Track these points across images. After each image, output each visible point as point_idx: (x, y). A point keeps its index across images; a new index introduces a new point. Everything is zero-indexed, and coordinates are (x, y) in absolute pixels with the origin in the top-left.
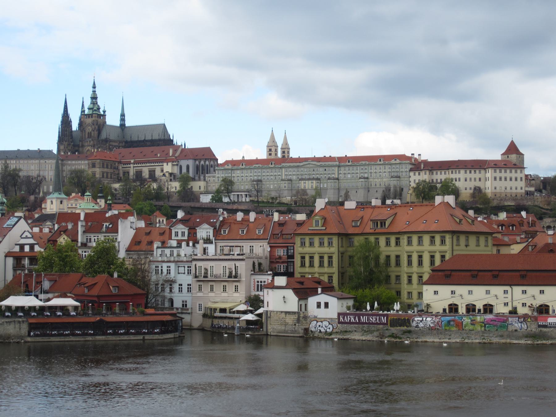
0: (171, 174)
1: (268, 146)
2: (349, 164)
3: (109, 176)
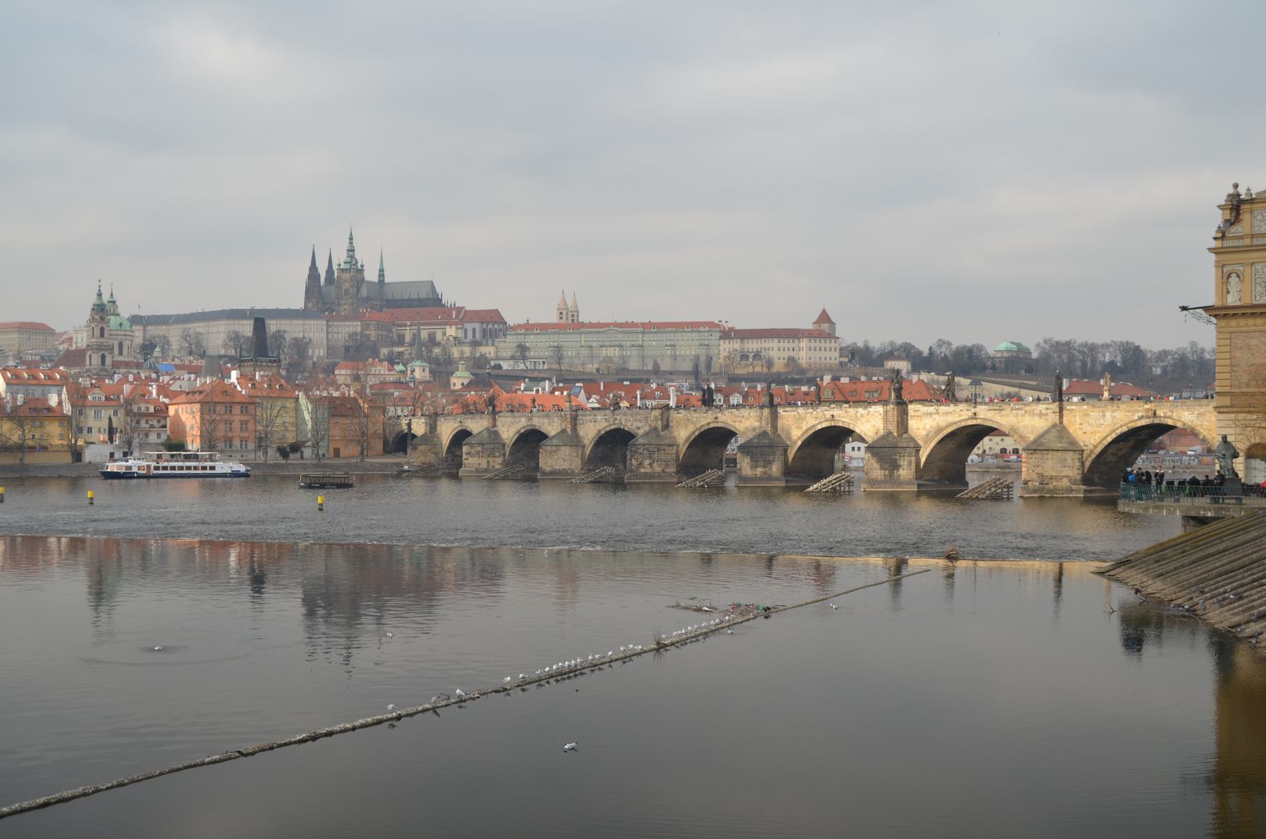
0: (455, 338)
1: (558, 309)
2: (654, 330)
3: (384, 338)
